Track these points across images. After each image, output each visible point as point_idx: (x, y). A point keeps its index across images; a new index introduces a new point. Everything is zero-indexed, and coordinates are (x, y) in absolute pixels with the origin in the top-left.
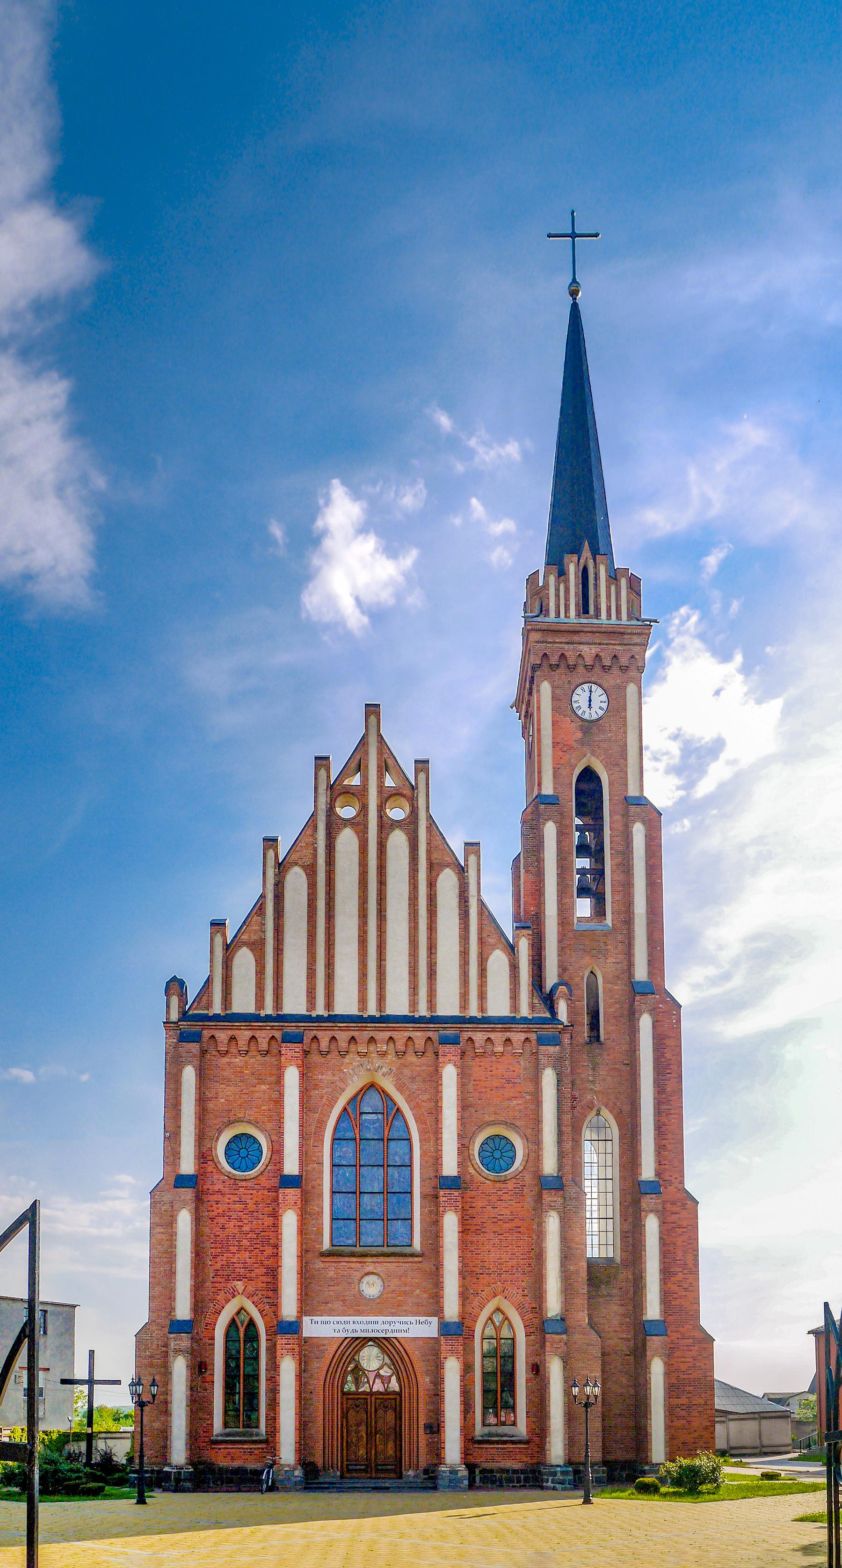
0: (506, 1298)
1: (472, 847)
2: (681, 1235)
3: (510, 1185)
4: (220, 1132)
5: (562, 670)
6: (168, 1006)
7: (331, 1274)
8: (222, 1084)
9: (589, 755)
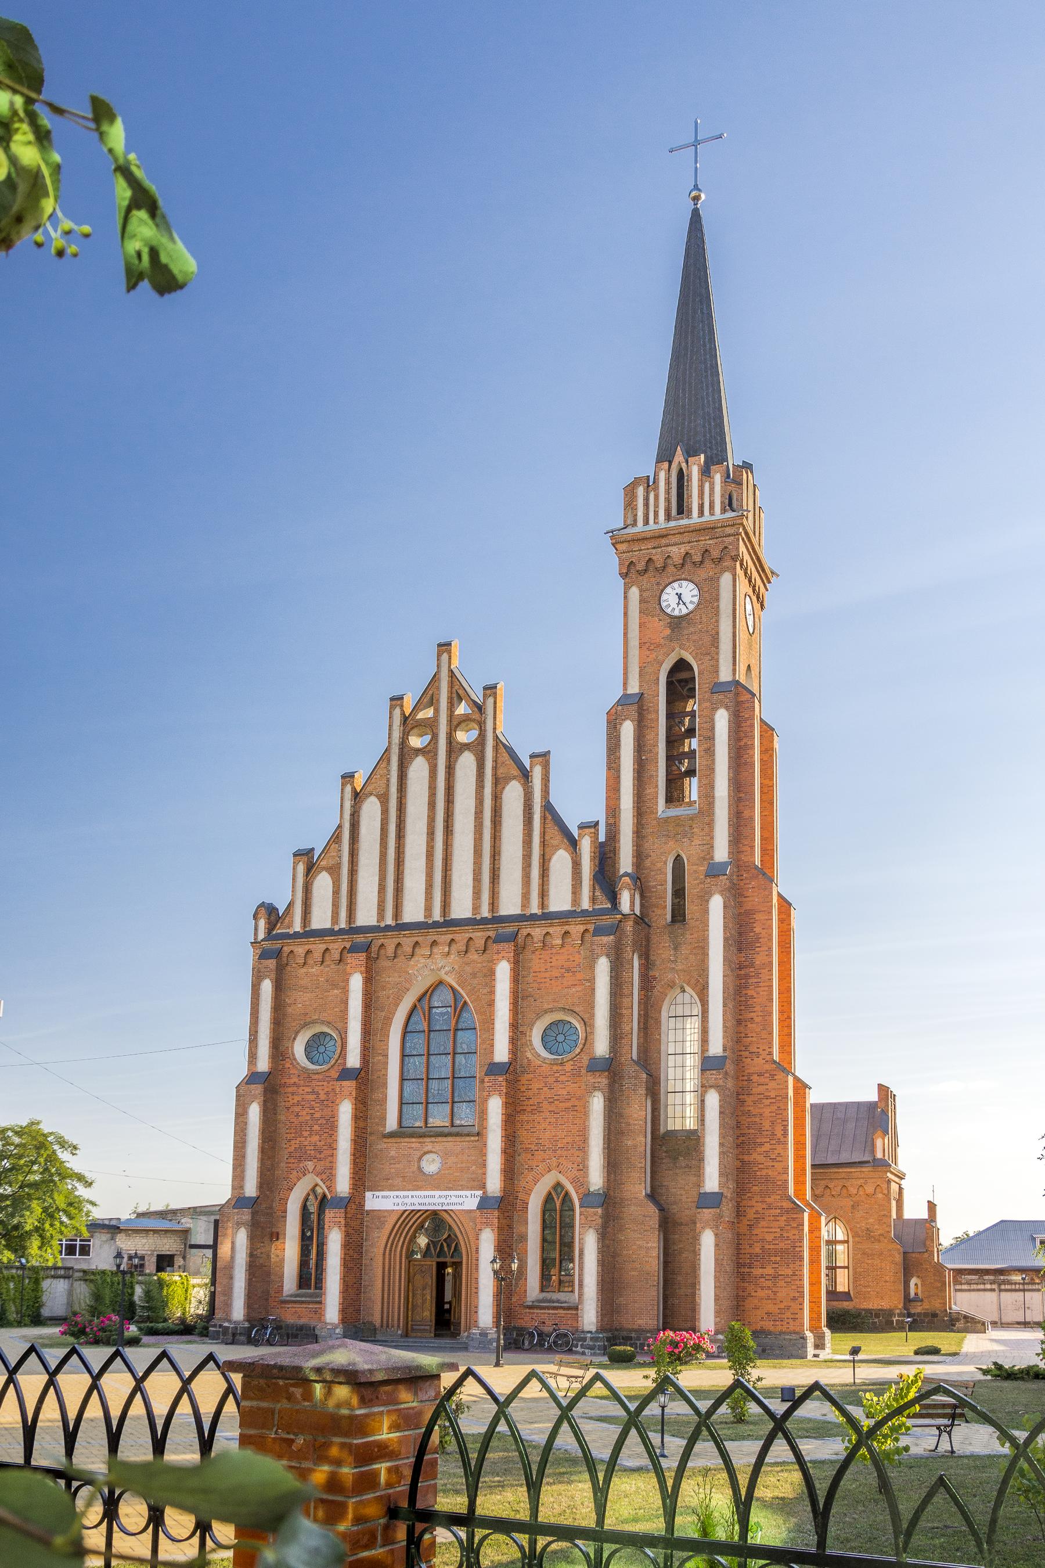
0: (560, 1172)
1: (543, 758)
2: (769, 1105)
3: (568, 1067)
4: (297, 1033)
5: (650, 574)
6: (256, 929)
7: (393, 1153)
8: (299, 991)
9: (677, 649)
